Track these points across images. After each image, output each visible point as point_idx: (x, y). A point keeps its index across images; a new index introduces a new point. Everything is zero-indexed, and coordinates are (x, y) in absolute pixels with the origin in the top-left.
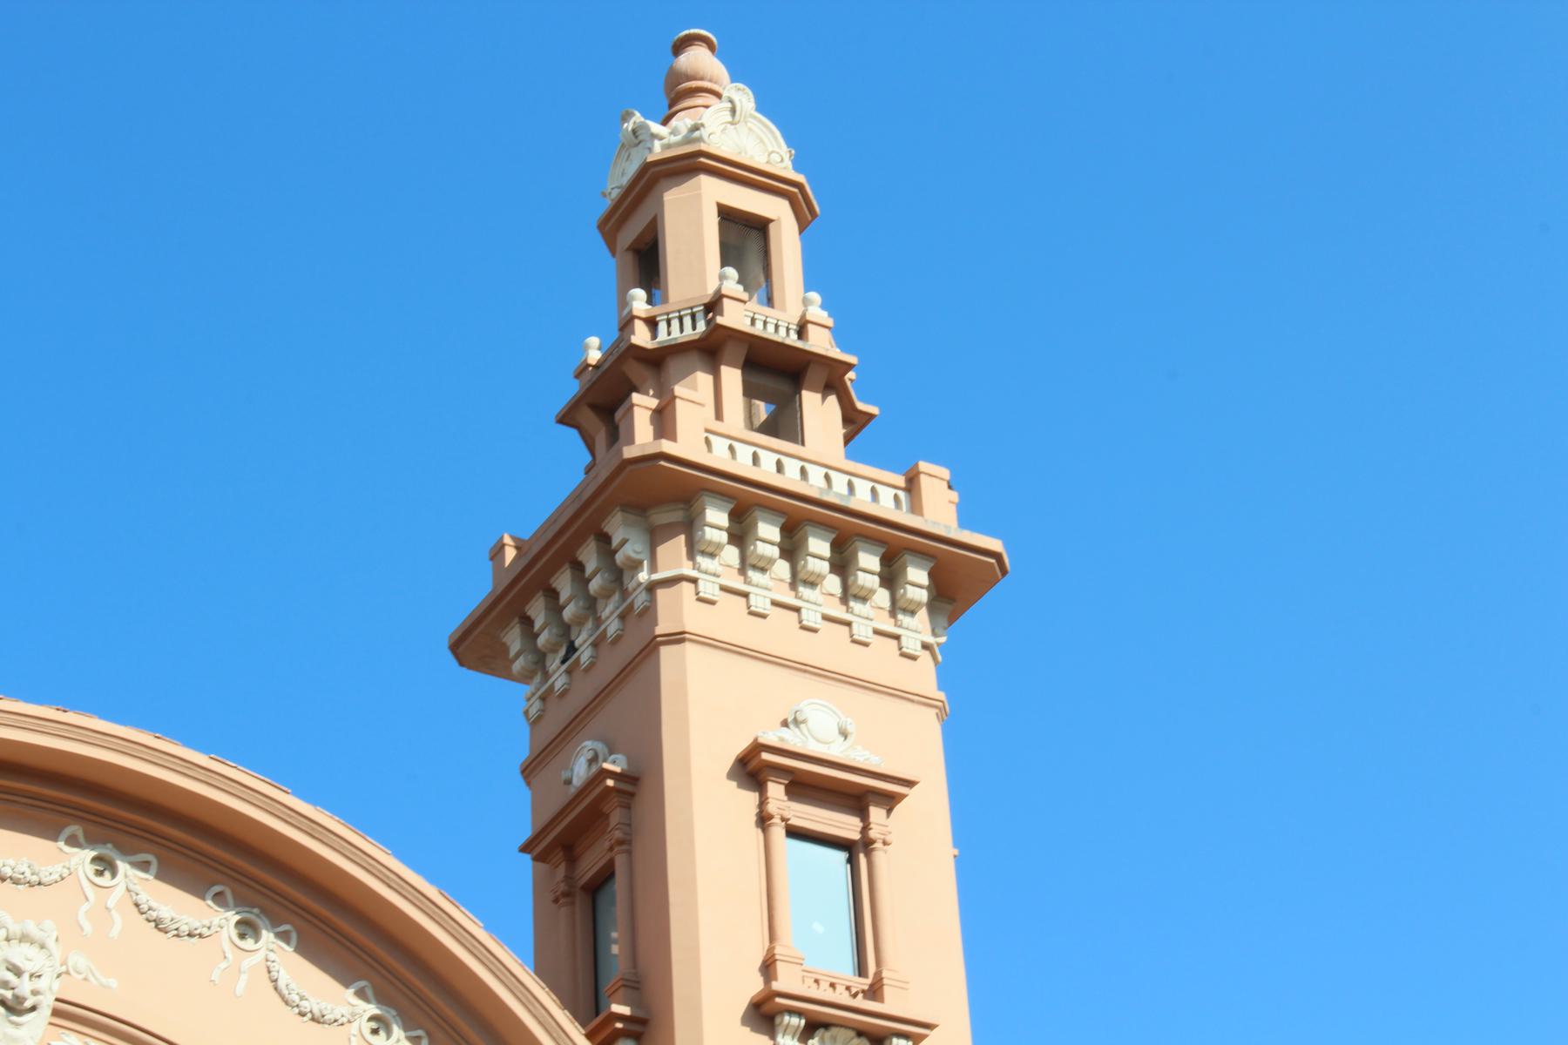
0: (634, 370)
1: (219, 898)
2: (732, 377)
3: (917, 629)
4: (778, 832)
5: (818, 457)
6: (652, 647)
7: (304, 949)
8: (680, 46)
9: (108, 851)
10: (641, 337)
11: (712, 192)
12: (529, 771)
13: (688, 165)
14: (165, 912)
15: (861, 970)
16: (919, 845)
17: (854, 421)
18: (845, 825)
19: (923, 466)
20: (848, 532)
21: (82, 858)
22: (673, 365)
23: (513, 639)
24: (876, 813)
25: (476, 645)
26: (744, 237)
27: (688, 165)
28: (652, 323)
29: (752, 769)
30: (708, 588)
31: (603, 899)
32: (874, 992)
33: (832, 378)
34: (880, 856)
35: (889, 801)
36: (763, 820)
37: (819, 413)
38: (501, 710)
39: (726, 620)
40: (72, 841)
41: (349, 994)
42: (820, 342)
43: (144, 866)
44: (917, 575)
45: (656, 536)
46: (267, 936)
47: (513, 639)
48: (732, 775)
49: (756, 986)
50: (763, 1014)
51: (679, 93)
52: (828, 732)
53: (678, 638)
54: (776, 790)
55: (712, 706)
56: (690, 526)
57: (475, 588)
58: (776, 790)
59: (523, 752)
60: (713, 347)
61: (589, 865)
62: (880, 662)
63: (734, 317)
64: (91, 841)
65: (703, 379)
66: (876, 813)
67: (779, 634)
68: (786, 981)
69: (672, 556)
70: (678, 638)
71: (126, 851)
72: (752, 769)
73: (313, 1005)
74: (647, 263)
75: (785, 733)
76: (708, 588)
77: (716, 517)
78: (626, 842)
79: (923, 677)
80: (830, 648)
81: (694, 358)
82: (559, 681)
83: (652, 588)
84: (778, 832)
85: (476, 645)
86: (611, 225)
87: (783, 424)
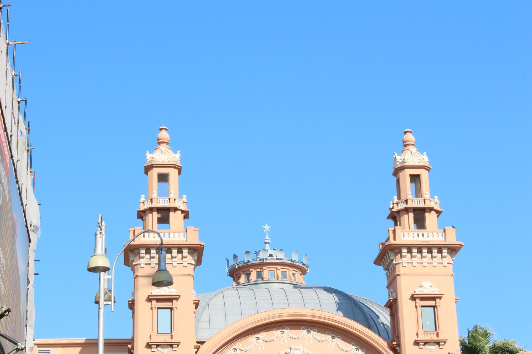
1: (328, 334)
2: (411, 215)
3: (448, 259)
4: (419, 308)
6: (395, 277)
7: (343, 339)
8: (405, 133)
9: (309, 330)
10: (396, 209)
11: (408, 172)
12: (388, 287)
13: (402, 168)
14: (319, 338)
15: (436, 330)
17: (438, 213)
18: (432, 303)
19: (446, 228)
20: (430, 248)
21: (305, 332)
22: (401, 213)
24: (438, 300)
25: (378, 262)
27: (402, 168)
29: (413, 298)
30: (405, 264)
32: (438, 335)
33: (431, 209)
34: (439, 308)
35: (440, 298)
36: (416, 307)
37: (430, 218)
39: (409, 269)
40: (303, 329)
41: (351, 345)
42: (428, 204)
43: (315, 331)
44: (445, 251)
45: (396, 254)
46: (336, 338)
47: (382, 263)
48: (410, 299)
49: (415, 338)
50: (417, 343)
52: (427, 288)
53: (399, 275)
54: (418, 300)
55: (406, 287)
56: (401, 252)
58: (418, 300)
59: (386, 284)
60: (407, 210)
62: (440, 269)
63: (411, 204)
64: (306, 329)
65: (406, 216)
66: (437, 300)
67: (419, 269)
69: (397, 259)
70: (399, 275)
71: (311, 329)
72: (413, 298)
73: (345, 349)
75: (420, 289)
76: (405, 264)
77: (404, 251)
79: (450, 269)
80: (430, 269)
81: (404, 212)
83: (395, 264)
84: (419, 308)
85: (378, 262)
87: (420, 223)
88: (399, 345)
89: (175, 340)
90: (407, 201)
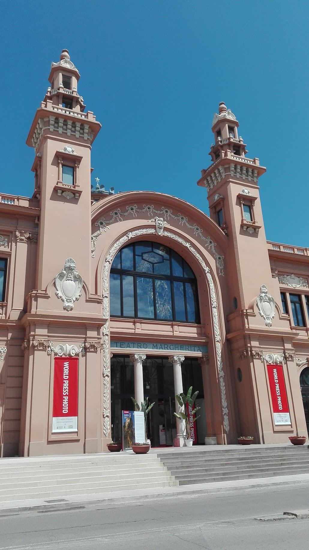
0: (219, 148)
5: (242, 159)
12: (208, 198)
16: (257, 207)
23: (205, 182)
26: (231, 129)
28: (221, 141)
31: (220, 214)
32: (254, 223)
38: (204, 191)
51: (221, 110)
57: (200, 176)
61: (218, 209)
68: (245, 222)
74: (219, 133)
78: (223, 206)
82: (212, 187)
85: (200, 183)
86: (213, 128)
88: (227, 228)
89: (77, 189)
90: (229, 139)
